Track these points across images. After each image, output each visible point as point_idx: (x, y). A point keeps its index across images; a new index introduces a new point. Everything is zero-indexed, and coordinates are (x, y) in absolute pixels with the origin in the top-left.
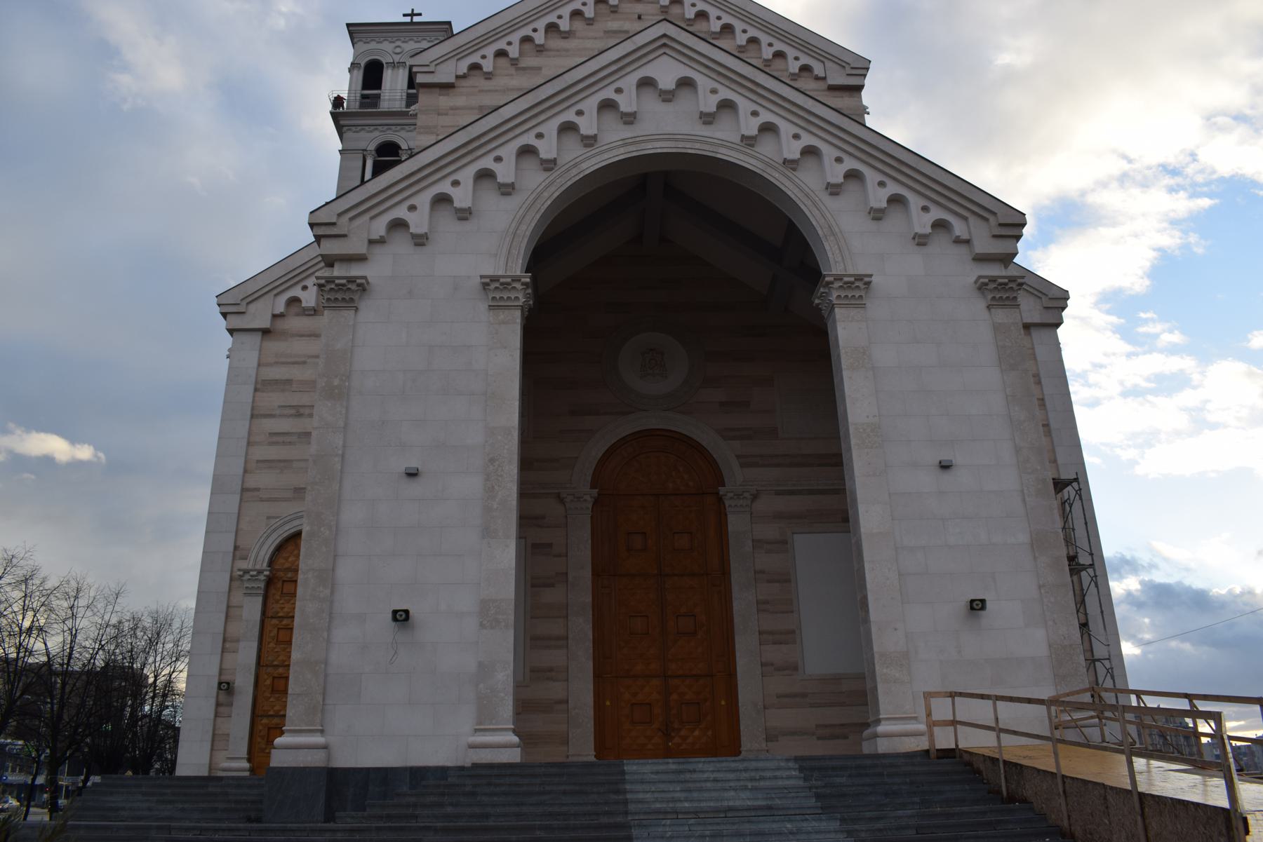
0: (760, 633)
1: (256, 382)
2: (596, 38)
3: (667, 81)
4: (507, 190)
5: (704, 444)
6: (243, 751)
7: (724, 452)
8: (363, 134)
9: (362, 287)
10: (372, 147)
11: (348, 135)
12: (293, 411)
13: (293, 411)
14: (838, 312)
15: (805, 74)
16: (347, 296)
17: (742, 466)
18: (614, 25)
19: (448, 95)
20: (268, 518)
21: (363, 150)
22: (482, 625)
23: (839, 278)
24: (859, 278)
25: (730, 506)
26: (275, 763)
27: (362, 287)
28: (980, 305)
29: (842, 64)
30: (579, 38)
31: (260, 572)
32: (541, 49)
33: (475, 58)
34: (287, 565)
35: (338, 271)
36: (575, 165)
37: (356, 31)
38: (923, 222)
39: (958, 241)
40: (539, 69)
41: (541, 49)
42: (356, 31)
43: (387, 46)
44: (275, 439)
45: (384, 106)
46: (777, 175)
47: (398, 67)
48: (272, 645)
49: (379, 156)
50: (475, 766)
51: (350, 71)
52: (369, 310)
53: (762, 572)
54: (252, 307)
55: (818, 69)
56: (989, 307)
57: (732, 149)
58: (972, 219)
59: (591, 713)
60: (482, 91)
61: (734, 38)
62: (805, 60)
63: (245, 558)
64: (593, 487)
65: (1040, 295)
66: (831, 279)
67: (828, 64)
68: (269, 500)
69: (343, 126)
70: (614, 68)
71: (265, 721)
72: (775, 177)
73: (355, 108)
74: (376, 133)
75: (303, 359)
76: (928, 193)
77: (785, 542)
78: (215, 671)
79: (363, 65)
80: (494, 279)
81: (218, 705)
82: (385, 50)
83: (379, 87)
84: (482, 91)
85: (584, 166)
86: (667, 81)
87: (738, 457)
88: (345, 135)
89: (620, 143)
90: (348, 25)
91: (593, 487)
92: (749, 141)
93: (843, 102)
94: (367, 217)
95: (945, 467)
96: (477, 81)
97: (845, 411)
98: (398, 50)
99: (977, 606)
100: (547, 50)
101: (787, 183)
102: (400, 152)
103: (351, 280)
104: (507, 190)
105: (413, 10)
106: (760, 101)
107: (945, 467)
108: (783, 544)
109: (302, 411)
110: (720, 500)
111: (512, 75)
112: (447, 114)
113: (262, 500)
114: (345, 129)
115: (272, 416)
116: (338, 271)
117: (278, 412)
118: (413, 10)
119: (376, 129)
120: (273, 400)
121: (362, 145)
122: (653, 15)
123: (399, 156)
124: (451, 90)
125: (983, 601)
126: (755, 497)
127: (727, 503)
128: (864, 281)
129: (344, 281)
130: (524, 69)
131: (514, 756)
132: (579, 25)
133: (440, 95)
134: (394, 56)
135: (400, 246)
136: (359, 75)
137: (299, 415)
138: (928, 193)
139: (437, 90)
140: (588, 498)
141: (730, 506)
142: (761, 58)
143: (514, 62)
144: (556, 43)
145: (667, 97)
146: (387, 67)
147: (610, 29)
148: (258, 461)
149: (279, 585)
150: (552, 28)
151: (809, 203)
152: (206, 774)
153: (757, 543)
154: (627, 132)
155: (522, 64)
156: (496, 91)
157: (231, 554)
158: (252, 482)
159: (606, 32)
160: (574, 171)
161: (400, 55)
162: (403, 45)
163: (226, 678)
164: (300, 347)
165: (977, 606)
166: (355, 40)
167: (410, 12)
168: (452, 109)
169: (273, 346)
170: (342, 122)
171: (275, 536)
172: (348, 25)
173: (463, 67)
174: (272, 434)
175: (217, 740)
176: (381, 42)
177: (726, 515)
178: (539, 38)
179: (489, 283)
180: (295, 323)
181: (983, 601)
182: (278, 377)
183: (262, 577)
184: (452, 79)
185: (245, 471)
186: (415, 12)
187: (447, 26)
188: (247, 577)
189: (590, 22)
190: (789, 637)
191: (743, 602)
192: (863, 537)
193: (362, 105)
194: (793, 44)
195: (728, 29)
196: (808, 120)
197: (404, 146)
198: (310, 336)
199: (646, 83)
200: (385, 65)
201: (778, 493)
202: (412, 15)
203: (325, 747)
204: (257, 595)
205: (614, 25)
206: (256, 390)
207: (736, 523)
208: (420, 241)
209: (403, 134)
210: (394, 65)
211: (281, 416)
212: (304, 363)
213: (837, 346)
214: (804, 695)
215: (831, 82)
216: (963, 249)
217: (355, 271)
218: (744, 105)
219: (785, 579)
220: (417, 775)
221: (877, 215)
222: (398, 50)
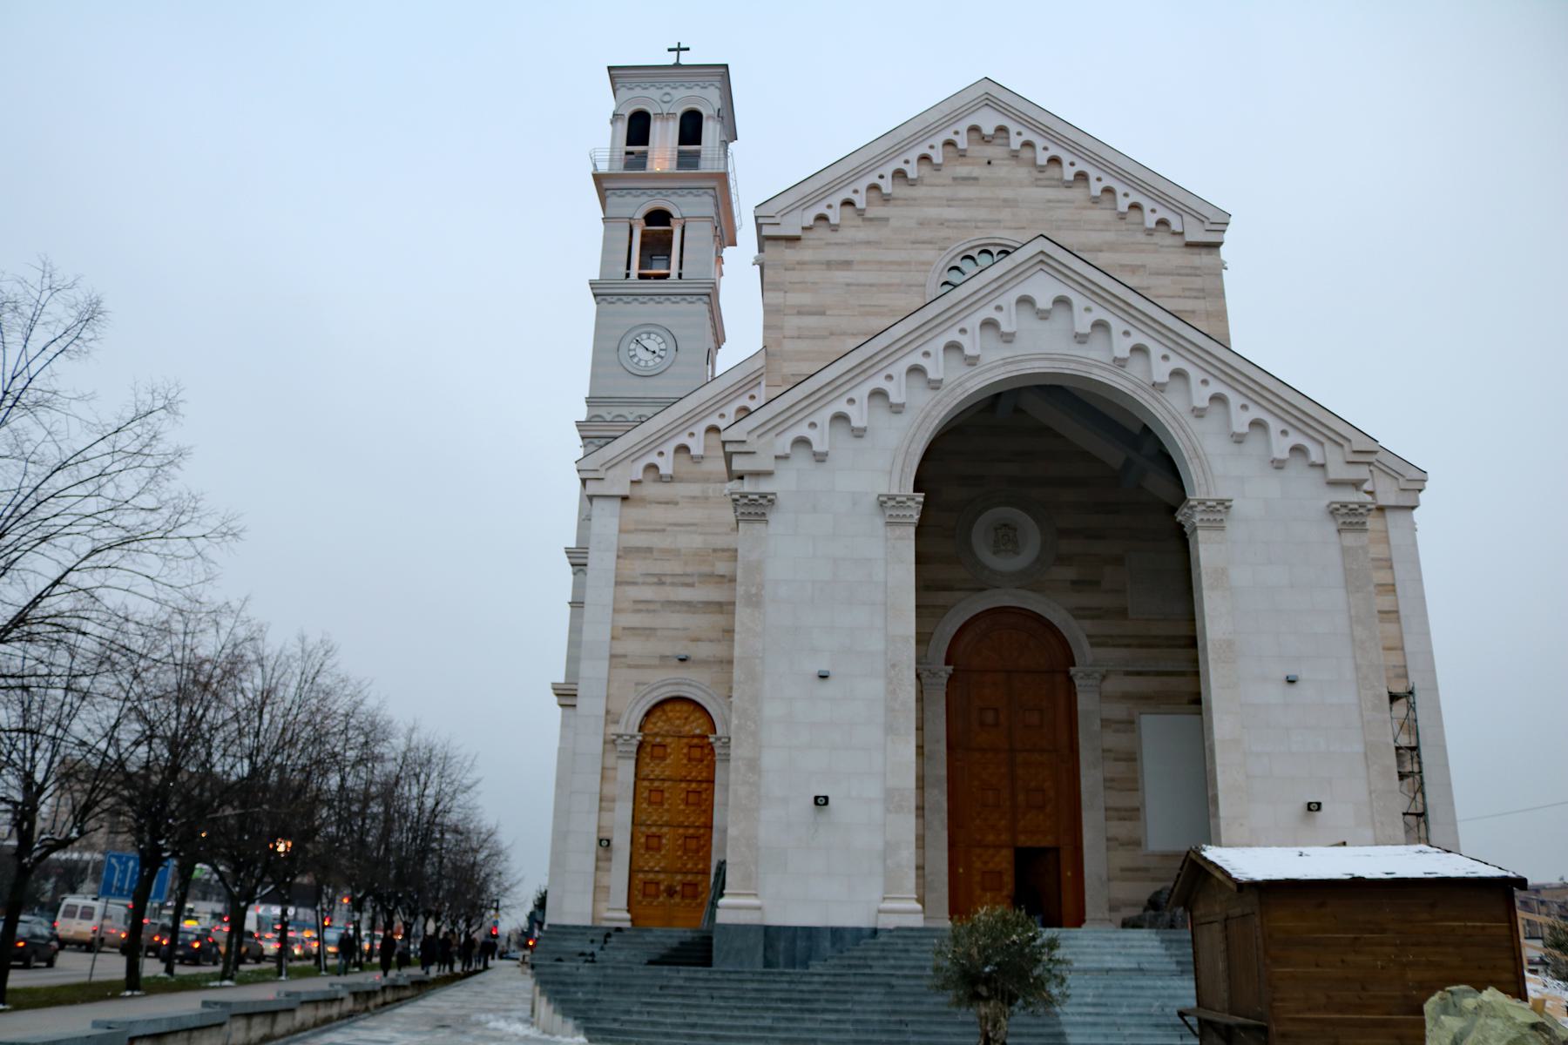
0: (1107, 809)
1: (618, 550)
2: (944, 186)
3: (1044, 301)
4: (897, 409)
5: (1055, 623)
6: (623, 903)
7: (1076, 632)
8: (629, 199)
9: (768, 500)
10: (640, 215)
11: (612, 200)
12: (655, 580)
13: (655, 580)
14: (1200, 533)
15: (1162, 228)
16: (759, 510)
17: (1092, 645)
18: (963, 171)
19: (794, 248)
20: (637, 684)
21: (630, 218)
22: (888, 810)
23: (1202, 502)
24: (1221, 502)
25: (1080, 686)
26: (722, 917)
27: (768, 500)
28: (1331, 528)
29: (1201, 219)
30: (926, 185)
31: (633, 737)
32: (887, 199)
33: (821, 209)
34: (656, 730)
35: (747, 486)
36: (960, 385)
37: (617, 74)
38: (1281, 447)
39: (1313, 465)
40: (886, 219)
41: (887, 199)
42: (617, 74)
43: (654, 93)
44: (640, 606)
46: (1147, 397)
47: (667, 119)
48: (645, 805)
50: (898, 929)
51: (612, 123)
52: (778, 521)
53: (1109, 751)
54: (610, 472)
55: (1176, 225)
56: (1339, 531)
57: (1104, 369)
58: (1328, 444)
59: (946, 879)
60: (828, 244)
61: (1088, 187)
62: (1163, 213)
63: (617, 722)
64: (947, 663)
65: (1397, 476)
66: (1195, 503)
67: (1187, 218)
68: (637, 667)
69: (607, 189)
70: (994, 285)
71: (641, 876)
72: (1144, 398)
73: (619, 168)
74: (644, 199)
75: (663, 527)
76: (1287, 417)
77: (1132, 722)
78: (594, 829)
80: (892, 498)
81: (598, 859)
82: (650, 99)
84: (828, 244)
85: (968, 385)
86: (1044, 301)
87: (1089, 636)
88: (609, 201)
89: (1001, 362)
90: (610, 68)
91: (947, 663)
92: (1120, 363)
93: (1202, 259)
94: (772, 434)
95: (1291, 681)
96: (822, 232)
97: (1204, 627)
98: (667, 98)
99: (1314, 807)
100: (895, 199)
101: (1156, 405)
102: (672, 220)
103: (763, 496)
104: (897, 409)
106: (1132, 321)
107: (1291, 681)
108: (1130, 724)
109: (664, 579)
110: (1070, 680)
111: (858, 227)
112: (794, 269)
113: (629, 667)
114: (608, 193)
115: (634, 583)
116: (747, 486)
117: (640, 580)
119: (644, 193)
120: (638, 567)
121: (627, 212)
122: (1003, 159)
123: (668, 224)
124: (798, 243)
125: (1319, 804)
126: (1104, 677)
127: (1077, 682)
128: (1225, 505)
129: (756, 497)
130: (871, 220)
131: (917, 921)
132: (926, 169)
133: (786, 248)
134: (663, 105)
135: (802, 460)
136: (623, 128)
137: (661, 583)
138: (1287, 417)
139: (783, 243)
140: (943, 674)
141: (1080, 686)
142: (1116, 209)
143: (861, 213)
144: (903, 191)
145: (1043, 315)
146: (655, 119)
147: (959, 175)
148: (624, 629)
149: (649, 749)
150: (900, 174)
151: (1175, 425)
152: (588, 922)
153: (1106, 723)
154: (1007, 352)
155: (868, 214)
156: (843, 244)
157: (603, 719)
158: (620, 648)
159: (955, 179)
160: (959, 391)
161: (670, 104)
162: (672, 92)
163: (605, 835)
164: (659, 515)
165: (1314, 807)
166: (618, 86)
167: (676, 46)
168: (798, 263)
169: (634, 513)
170: (606, 185)
171: (643, 702)
172: (610, 68)
173: (809, 219)
174: (636, 602)
175: (599, 891)
176: (646, 88)
177: (1075, 694)
178: (887, 186)
179: (883, 502)
180: (652, 490)
181: (1319, 804)
182: (639, 545)
183: (635, 742)
184: (797, 232)
185: (613, 638)
186: (682, 46)
187: (723, 70)
188: (620, 741)
189: (938, 168)
190: (1133, 814)
191: (1091, 778)
192: (1216, 743)
194: (1149, 194)
195: (1082, 177)
196: (1177, 343)
197: (676, 214)
198: (667, 503)
199: (1025, 301)
201: (1128, 673)
202: (679, 49)
203: (759, 908)
204: (630, 758)
205: (963, 171)
206: (618, 557)
207: (1085, 702)
208: (820, 458)
209: (674, 199)
210: (666, 117)
211: (644, 583)
212: (664, 530)
213: (1199, 566)
214: (1146, 870)
215: (1189, 238)
216: (1316, 474)
217: (765, 486)
218: (1117, 325)
219: (1132, 758)
220: (837, 933)
221: (1239, 439)
222: (667, 98)
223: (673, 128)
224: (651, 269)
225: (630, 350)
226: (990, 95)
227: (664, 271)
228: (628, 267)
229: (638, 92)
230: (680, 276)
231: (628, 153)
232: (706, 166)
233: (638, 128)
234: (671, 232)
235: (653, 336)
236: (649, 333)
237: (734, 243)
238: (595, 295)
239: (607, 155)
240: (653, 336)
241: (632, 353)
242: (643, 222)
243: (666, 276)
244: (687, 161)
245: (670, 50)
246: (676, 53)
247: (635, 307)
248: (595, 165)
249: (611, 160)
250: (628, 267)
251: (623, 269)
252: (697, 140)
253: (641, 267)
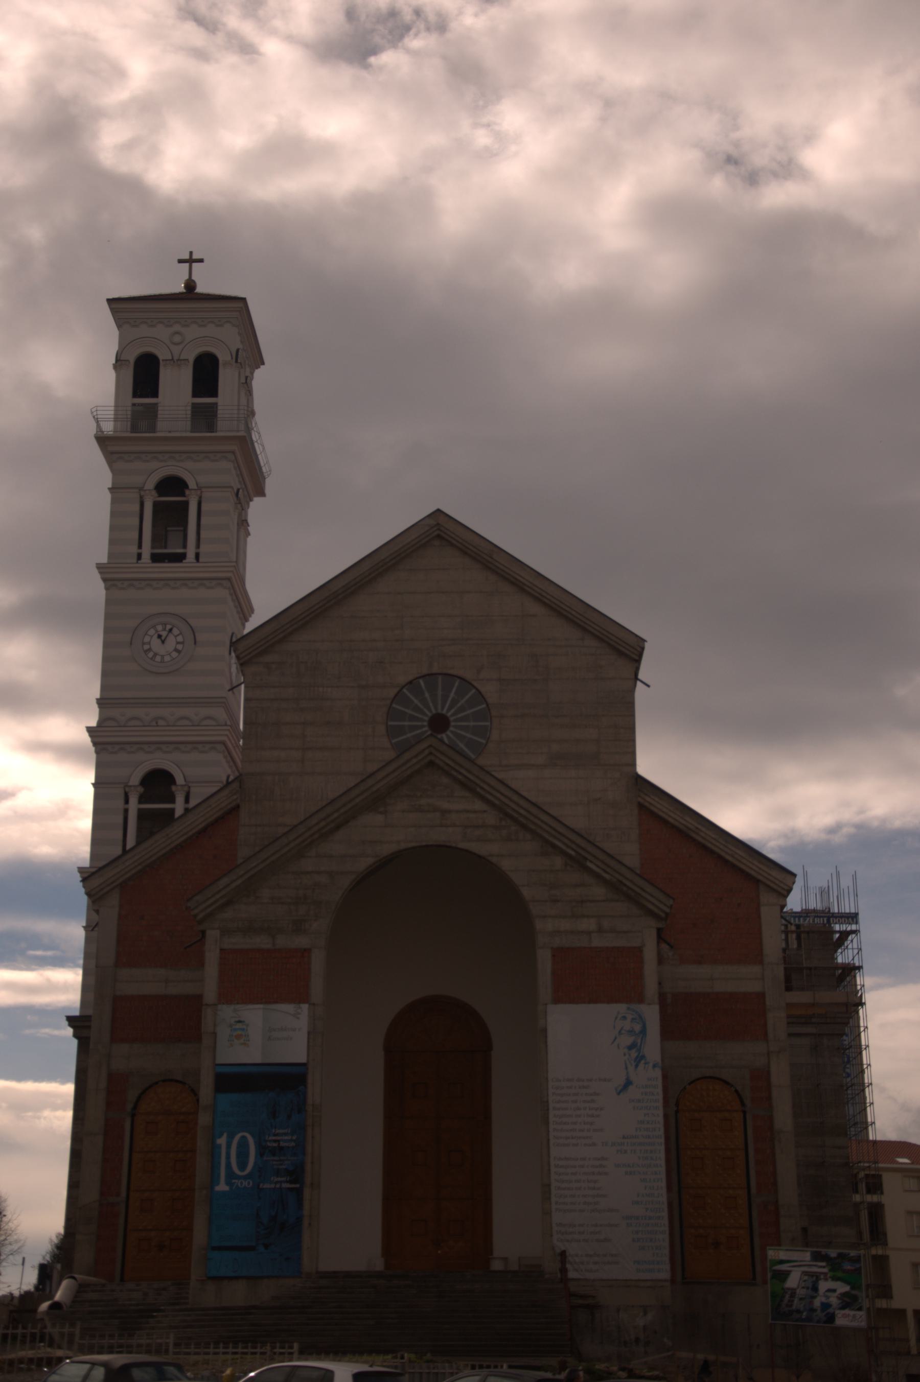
10: (151, 484)
45: (163, 427)
49: (160, 495)
79: (132, 361)
83: (155, 394)
90: (110, 301)
98: (177, 339)
105: (191, 253)
118: (191, 253)
123: (183, 495)
167: (187, 257)
172: (110, 301)
186: (195, 257)
187: (241, 305)
193: (134, 429)
197: (192, 484)
200: (161, 362)
202: (191, 261)
210: (176, 362)
222: (177, 339)
223: (186, 376)
224: (166, 548)
225: (144, 644)
226: (439, 511)
227: (181, 551)
228: (140, 546)
230: (197, 556)
231: (134, 405)
232: (224, 427)
234: (186, 504)
237: (262, 493)
238: (105, 580)
239: (111, 413)
241: (146, 647)
242: (154, 493)
243: (180, 558)
245: (180, 261)
246: (187, 265)
248: (98, 426)
249: (116, 420)
250: (140, 546)
251: (134, 549)
253: (157, 540)
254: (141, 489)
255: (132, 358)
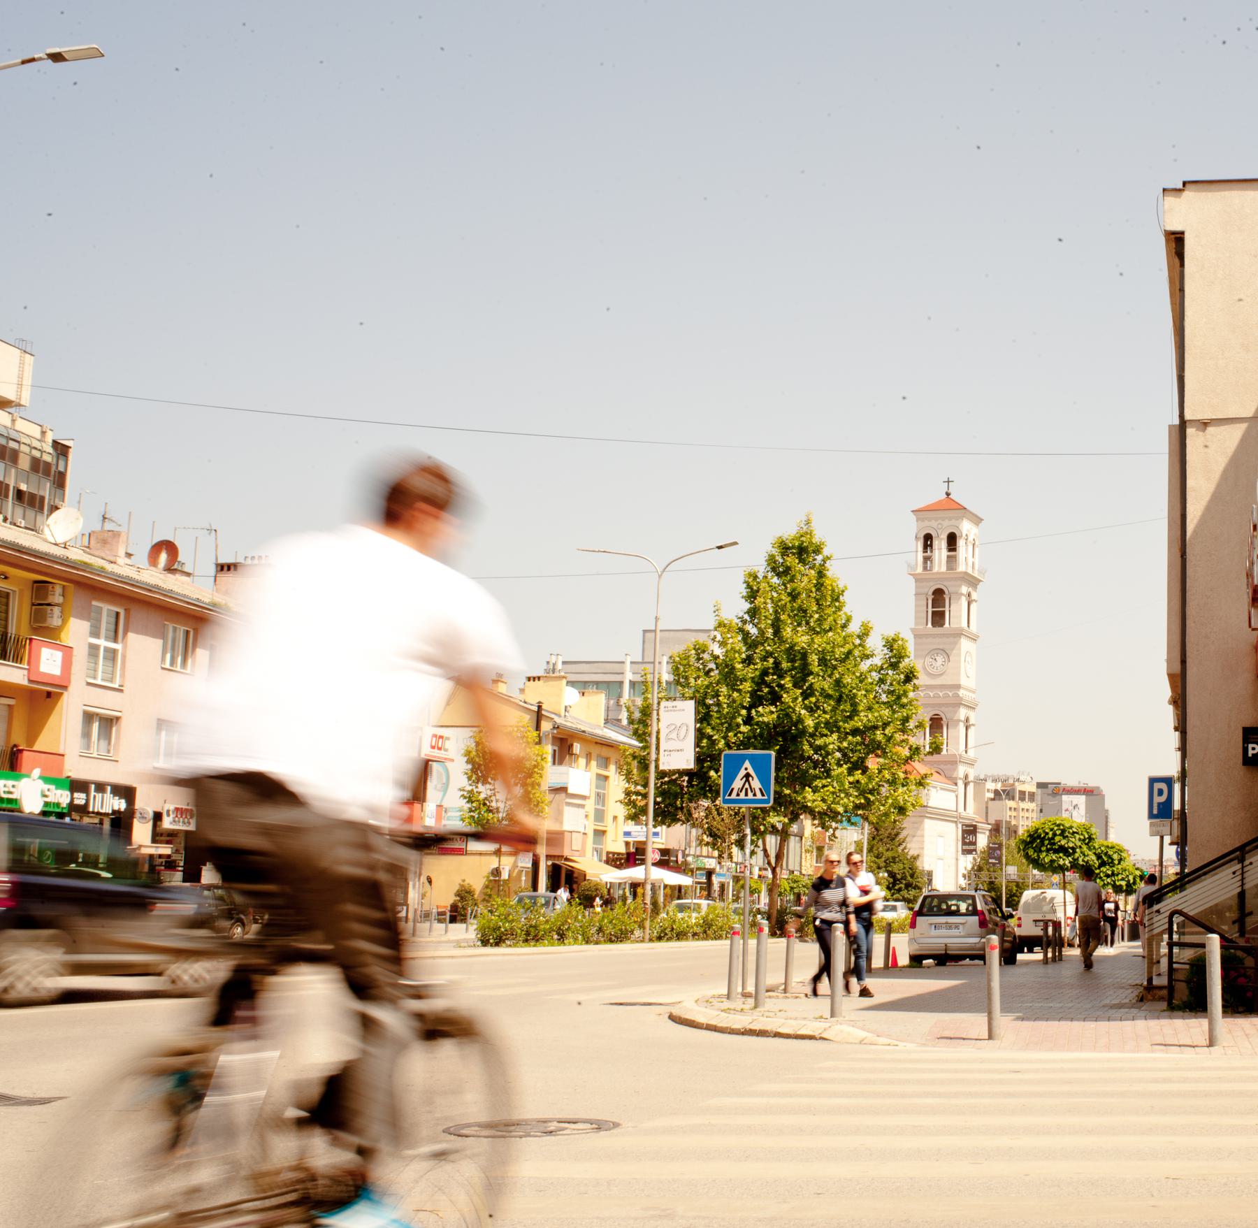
43: (934, 524)
74: (932, 584)
121: (925, 590)
162: (942, 522)
222: (940, 526)
223: (944, 544)
229: (927, 523)
233: (928, 540)
235: (939, 655)
236: (937, 654)
240: (939, 655)
244: (952, 561)
247: (930, 640)
252: (954, 550)
254: (927, 594)
255: (922, 535)
